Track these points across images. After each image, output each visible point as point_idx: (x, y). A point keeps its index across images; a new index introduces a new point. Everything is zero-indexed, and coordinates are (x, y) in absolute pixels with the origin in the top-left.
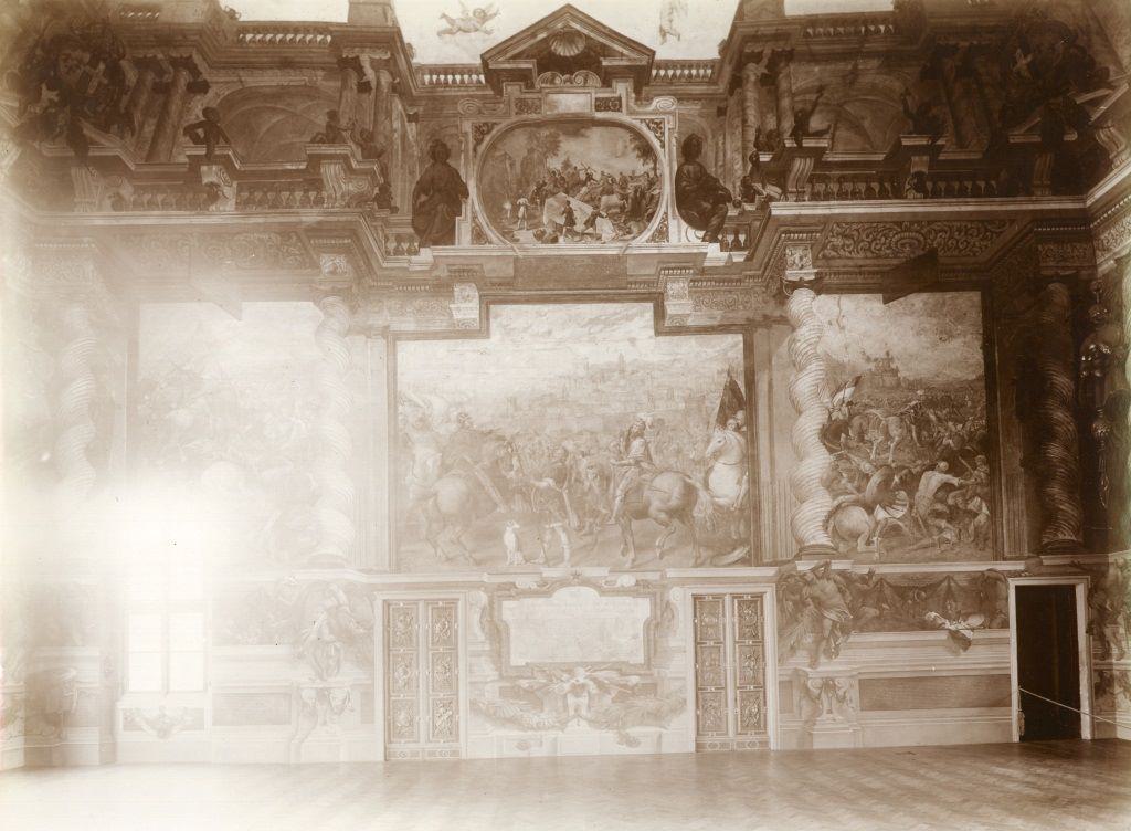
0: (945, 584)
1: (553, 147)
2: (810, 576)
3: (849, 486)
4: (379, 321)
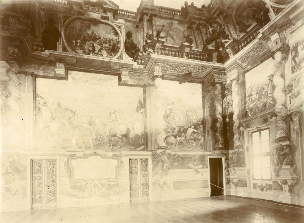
0: (193, 157)
1: (89, 27)
2: (160, 154)
3: (170, 131)
4: (31, 70)
